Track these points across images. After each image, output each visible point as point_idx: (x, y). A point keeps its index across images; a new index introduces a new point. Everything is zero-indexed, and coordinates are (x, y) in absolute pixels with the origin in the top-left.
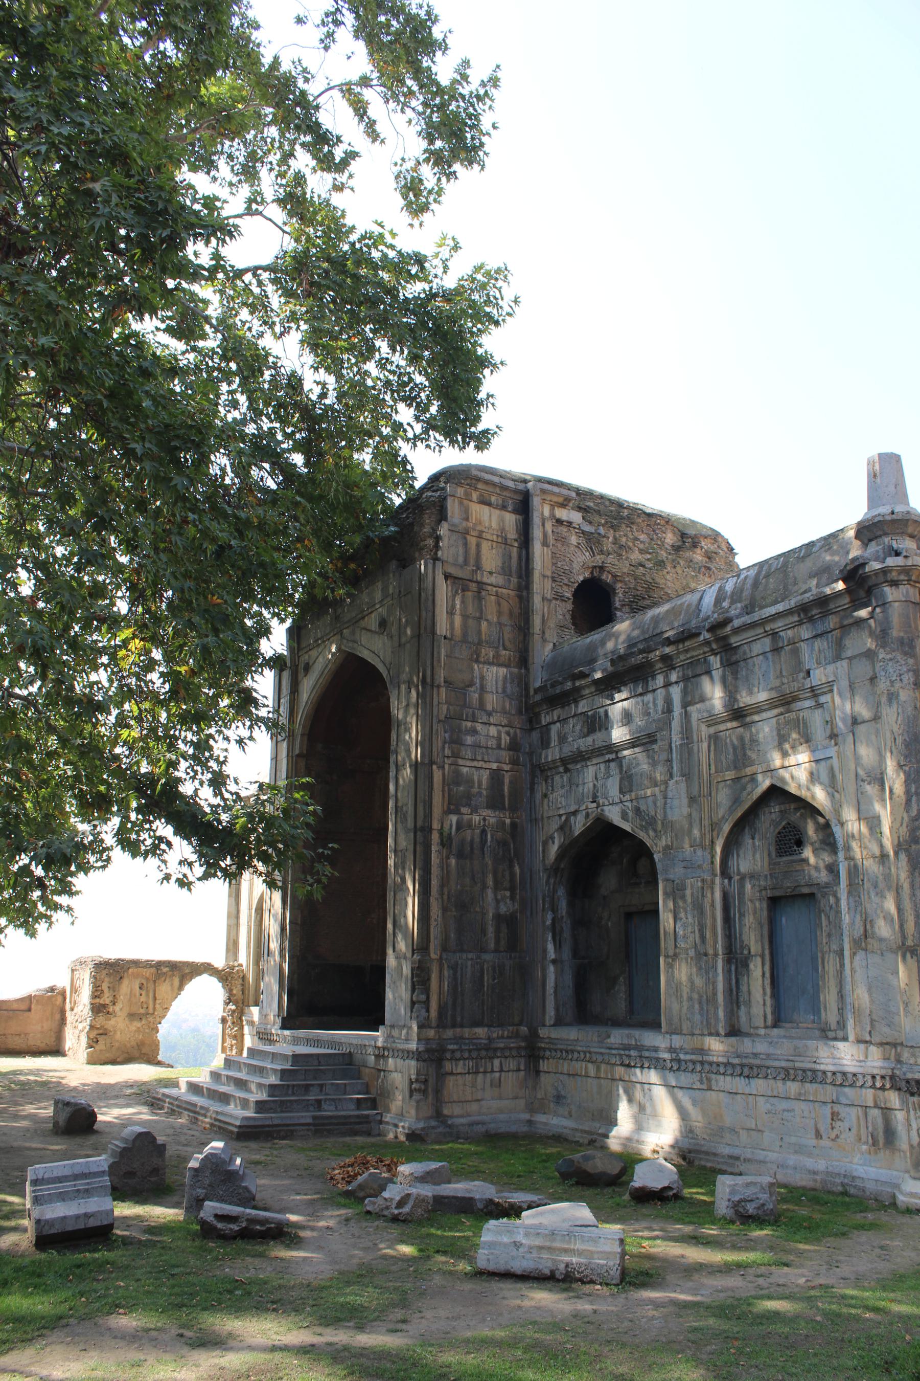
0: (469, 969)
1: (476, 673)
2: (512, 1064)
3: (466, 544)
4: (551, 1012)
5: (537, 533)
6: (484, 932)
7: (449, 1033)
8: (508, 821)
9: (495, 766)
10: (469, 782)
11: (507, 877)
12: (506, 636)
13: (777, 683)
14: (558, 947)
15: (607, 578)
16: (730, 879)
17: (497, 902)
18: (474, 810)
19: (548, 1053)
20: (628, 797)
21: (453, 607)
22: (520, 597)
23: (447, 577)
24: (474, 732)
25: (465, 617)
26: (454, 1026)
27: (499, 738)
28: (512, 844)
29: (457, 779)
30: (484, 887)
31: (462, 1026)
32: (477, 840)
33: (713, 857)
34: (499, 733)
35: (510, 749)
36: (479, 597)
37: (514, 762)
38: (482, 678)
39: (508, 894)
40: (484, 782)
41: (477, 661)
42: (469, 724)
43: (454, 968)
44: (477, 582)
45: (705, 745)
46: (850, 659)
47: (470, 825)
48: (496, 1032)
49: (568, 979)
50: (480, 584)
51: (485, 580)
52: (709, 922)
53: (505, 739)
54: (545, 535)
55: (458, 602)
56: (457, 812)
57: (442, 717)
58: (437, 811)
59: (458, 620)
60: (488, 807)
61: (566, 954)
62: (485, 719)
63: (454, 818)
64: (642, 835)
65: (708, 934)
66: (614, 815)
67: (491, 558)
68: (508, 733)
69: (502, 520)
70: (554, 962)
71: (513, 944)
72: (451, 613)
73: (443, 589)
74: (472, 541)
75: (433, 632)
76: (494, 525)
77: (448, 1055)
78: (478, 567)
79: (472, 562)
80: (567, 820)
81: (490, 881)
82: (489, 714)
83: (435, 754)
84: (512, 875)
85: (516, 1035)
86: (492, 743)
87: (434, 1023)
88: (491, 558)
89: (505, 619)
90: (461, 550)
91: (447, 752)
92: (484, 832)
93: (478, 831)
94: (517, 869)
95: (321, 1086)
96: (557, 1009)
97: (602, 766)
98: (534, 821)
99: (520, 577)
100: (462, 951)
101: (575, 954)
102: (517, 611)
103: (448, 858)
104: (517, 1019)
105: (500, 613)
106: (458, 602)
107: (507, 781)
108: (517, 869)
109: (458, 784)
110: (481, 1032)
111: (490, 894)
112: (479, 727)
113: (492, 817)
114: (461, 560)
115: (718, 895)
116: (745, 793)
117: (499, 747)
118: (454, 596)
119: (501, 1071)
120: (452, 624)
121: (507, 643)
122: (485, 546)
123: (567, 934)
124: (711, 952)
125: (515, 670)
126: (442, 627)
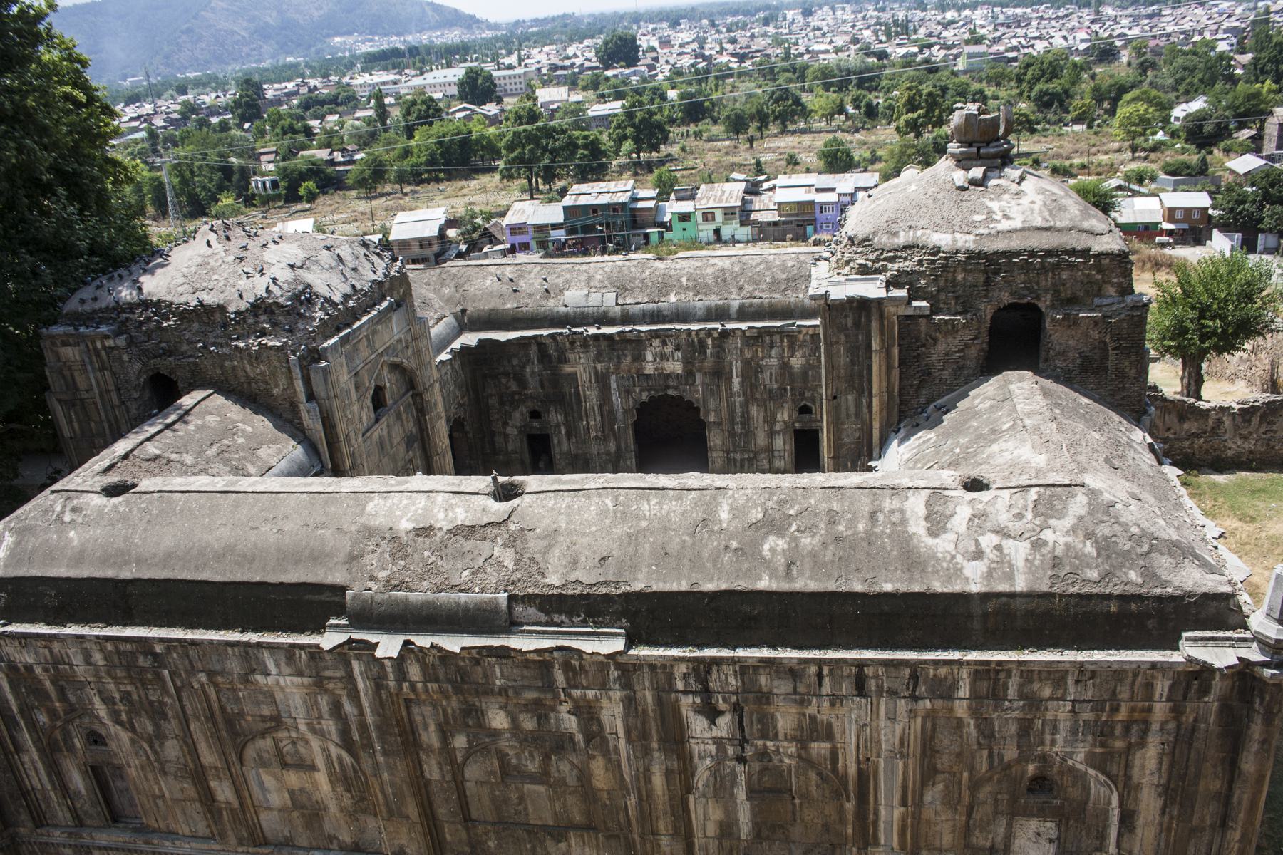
3: (64, 377)
23: (59, 401)
25: (80, 422)
50: (82, 400)
54: (102, 361)
59: (76, 425)
72: (70, 422)
74: (67, 373)
78: (77, 389)
126: (67, 432)
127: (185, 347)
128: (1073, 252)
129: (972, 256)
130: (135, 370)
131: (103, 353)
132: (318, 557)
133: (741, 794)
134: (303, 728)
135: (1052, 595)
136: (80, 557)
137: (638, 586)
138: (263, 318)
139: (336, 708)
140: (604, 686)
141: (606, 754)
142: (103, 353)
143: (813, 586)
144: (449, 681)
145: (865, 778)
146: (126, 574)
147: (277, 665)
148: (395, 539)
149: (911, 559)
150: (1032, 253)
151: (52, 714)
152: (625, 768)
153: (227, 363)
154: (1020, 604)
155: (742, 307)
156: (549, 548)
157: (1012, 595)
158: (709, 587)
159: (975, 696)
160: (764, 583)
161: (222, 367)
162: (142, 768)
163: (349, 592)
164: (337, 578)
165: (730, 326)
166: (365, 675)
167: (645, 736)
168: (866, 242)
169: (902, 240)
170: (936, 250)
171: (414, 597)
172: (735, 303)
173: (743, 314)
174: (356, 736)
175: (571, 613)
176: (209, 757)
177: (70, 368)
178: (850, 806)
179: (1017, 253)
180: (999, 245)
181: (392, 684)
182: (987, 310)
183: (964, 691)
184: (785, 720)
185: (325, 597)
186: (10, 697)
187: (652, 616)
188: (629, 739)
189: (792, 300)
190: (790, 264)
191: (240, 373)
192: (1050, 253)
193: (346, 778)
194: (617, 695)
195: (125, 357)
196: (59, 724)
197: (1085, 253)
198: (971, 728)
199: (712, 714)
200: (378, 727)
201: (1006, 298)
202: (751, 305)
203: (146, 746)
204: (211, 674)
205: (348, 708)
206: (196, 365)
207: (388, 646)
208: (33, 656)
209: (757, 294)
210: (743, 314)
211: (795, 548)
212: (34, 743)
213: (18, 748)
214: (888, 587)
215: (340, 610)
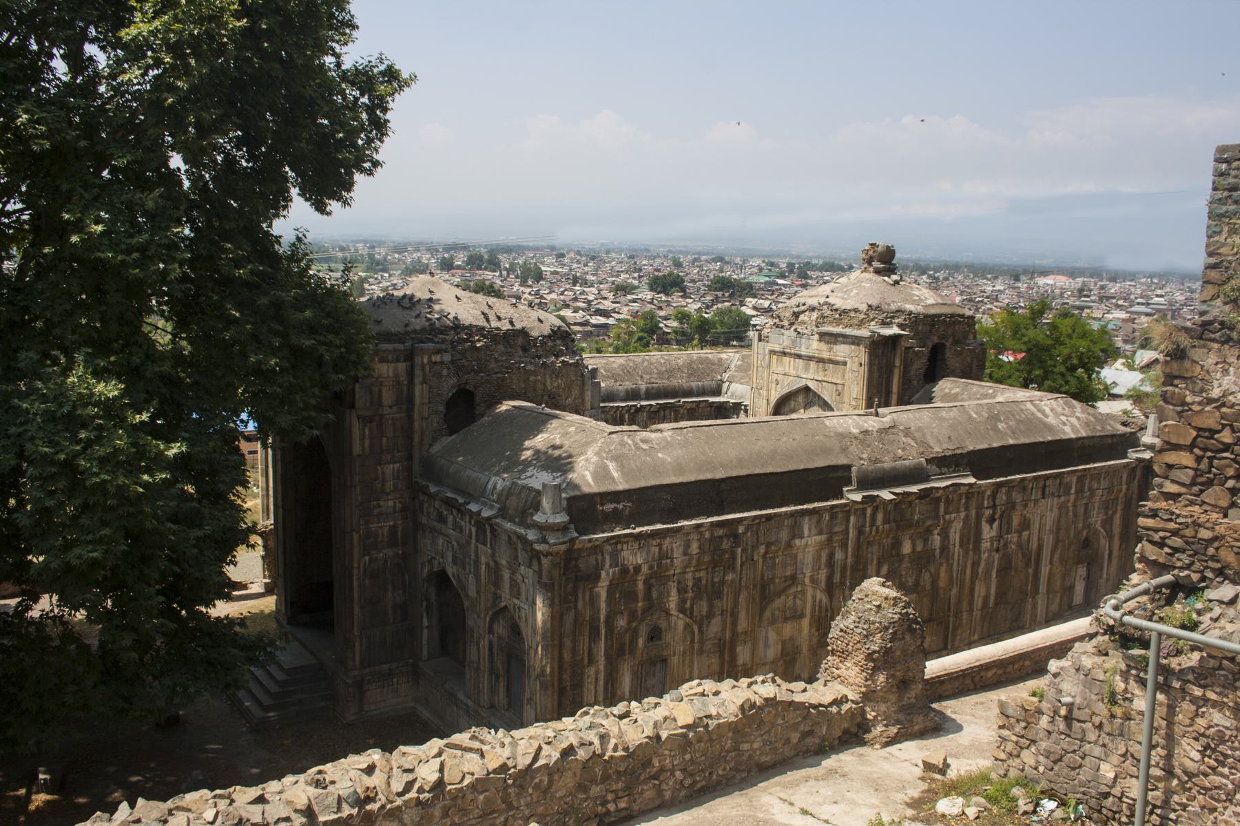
5: (418, 372)
7: (367, 671)
24: (379, 506)
38: (383, 473)
47: (377, 559)
50: (382, 416)
53: (399, 506)
54: (424, 375)
58: (356, 556)
59: (367, 442)
63: (367, 558)
67: (388, 397)
69: (396, 369)
72: (362, 439)
73: (356, 426)
74: (376, 389)
76: (391, 374)
78: (380, 404)
81: (390, 587)
82: (388, 494)
88: (388, 397)
91: (362, 522)
92: (386, 561)
110: (385, 667)
111: (390, 594)
112: (382, 503)
113: (390, 552)
115: (487, 643)
117: (395, 511)
120: (363, 446)
122: (384, 389)
126: (357, 449)
127: (493, 365)
128: (959, 315)
129: (926, 316)
130: (449, 385)
131: (427, 368)
132: (826, 451)
133: (994, 574)
134: (807, 581)
135: (1092, 437)
136: (680, 469)
137: (971, 448)
138: (559, 342)
139: (831, 556)
140: (958, 511)
141: (947, 561)
142: (427, 368)
143: (1027, 441)
144: (895, 521)
145: (1040, 547)
146: (720, 475)
147: (810, 529)
148: (856, 438)
149: (1050, 428)
150: (946, 315)
151: (632, 616)
152: (955, 568)
153: (532, 378)
154: (1087, 442)
155: (647, 389)
156: (924, 435)
157: (1083, 438)
158: (995, 445)
159: (1076, 492)
160: (1011, 442)
162: (684, 652)
163: (854, 469)
164: (843, 461)
165: (644, 403)
166: (855, 527)
167: (968, 543)
168: (878, 308)
169: (893, 307)
170: (911, 313)
171: (887, 466)
172: (643, 387)
173: (649, 395)
174: (837, 578)
175: (948, 466)
176: (743, 624)
177: (381, 384)
178: (1030, 571)
179: (940, 315)
180: (933, 311)
181: (867, 529)
182: (930, 345)
183: (1073, 491)
184: (1016, 521)
185: (839, 474)
186: (603, 605)
187: (981, 462)
188: (961, 546)
191: (540, 386)
192: (952, 316)
193: (819, 618)
194: (963, 515)
195: (445, 372)
196: (634, 624)
197: (962, 316)
198: (1071, 514)
199: (991, 521)
200: (852, 566)
201: (936, 340)
203: (696, 629)
204: (769, 545)
205: (839, 555)
206: (504, 379)
207: (886, 495)
210: (649, 395)
211: (1009, 427)
212: (606, 650)
213: (591, 661)
214: (1050, 438)
215: (849, 483)
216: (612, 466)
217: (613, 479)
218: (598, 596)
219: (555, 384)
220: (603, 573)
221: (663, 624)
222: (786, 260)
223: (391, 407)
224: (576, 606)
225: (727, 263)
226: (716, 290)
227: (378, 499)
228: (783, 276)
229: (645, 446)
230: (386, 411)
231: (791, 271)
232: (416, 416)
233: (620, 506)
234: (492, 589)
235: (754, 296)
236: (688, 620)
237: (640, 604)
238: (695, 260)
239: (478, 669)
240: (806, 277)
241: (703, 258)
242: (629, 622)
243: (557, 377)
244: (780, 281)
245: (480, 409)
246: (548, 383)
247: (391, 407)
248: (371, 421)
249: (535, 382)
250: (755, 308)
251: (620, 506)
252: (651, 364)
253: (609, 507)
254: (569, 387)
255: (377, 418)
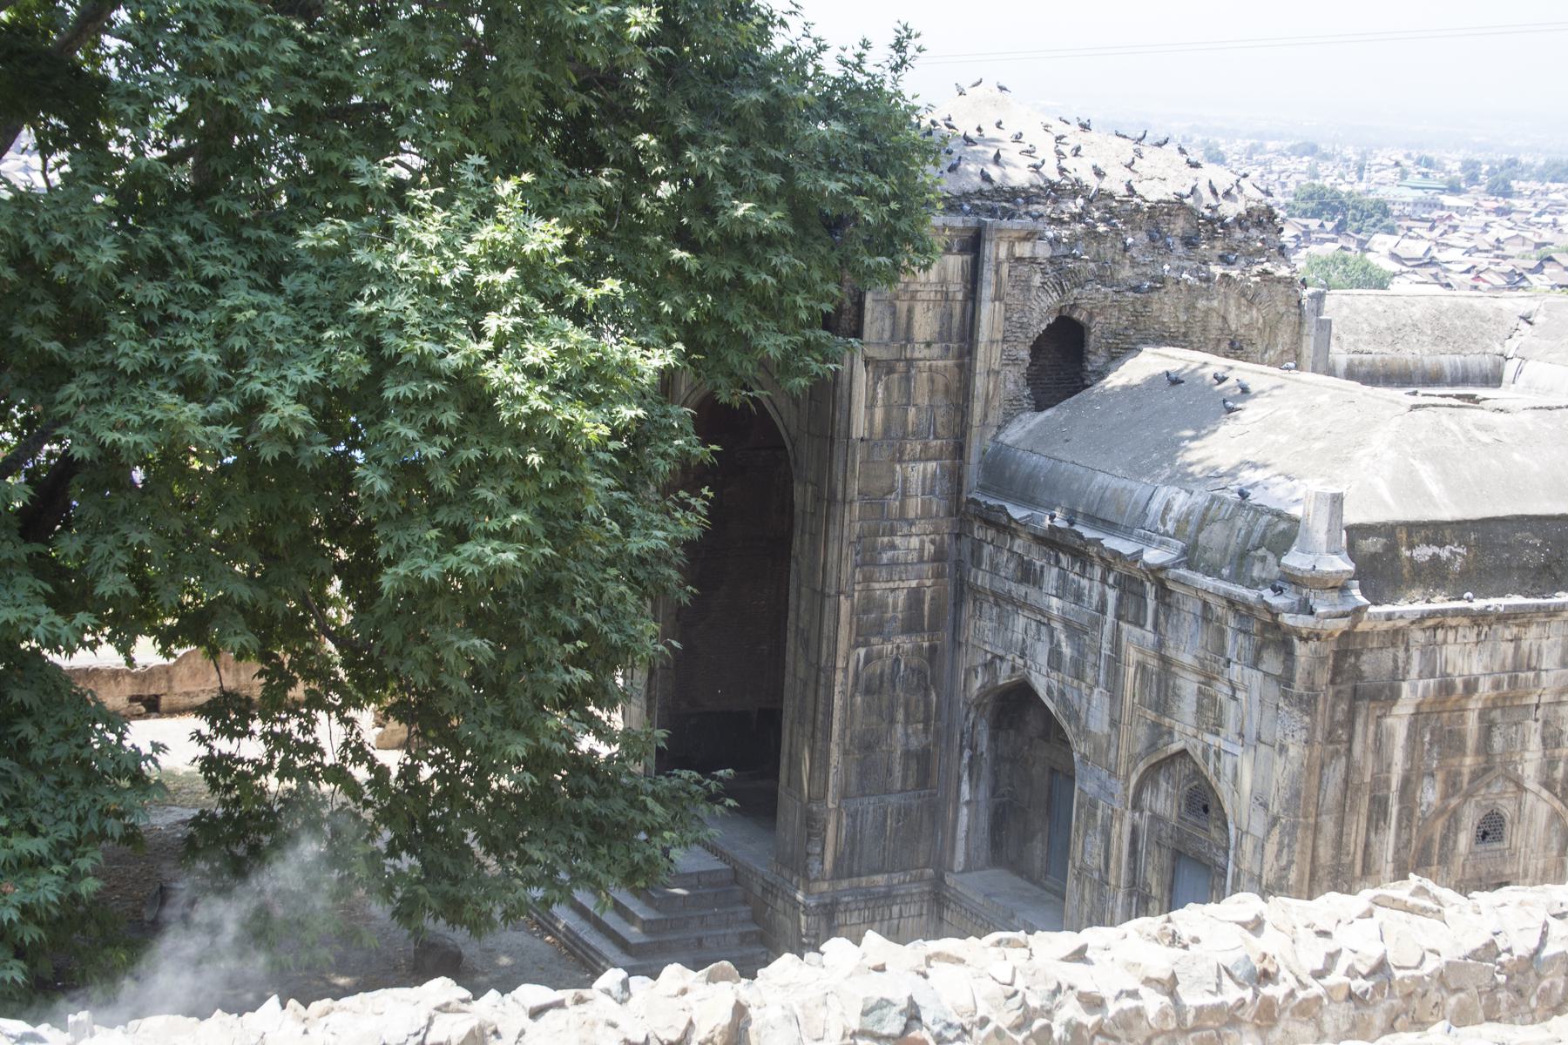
0: (870, 817)
1: (898, 477)
2: (914, 909)
3: (894, 313)
4: (960, 857)
5: (988, 275)
6: (889, 772)
7: (845, 884)
8: (926, 644)
9: (914, 584)
10: (883, 606)
11: (922, 708)
12: (939, 420)
13: (1201, 654)
14: (974, 787)
15: (1080, 316)
16: (1142, 812)
17: (907, 735)
18: (887, 639)
19: (952, 906)
20: (1054, 674)
21: (874, 398)
22: (960, 367)
24: (893, 547)
25: (888, 407)
26: (850, 875)
27: (922, 549)
28: (932, 671)
29: (869, 604)
30: (892, 721)
31: (859, 875)
32: (887, 671)
33: (1126, 789)
34: (922, 543)
35: (933, 561)
36: (907, 378)
37: (938, 575)
38: (905, 480)
39: (920, 726)
40: (900, 604)
41: (900, 461)
42: (886, 539)
43: (853, 816)
44: (906, 360)
45: (1132, 670)
46: (1266, 674)
47: (880, 657)
48: (897, 878)
49: (984, 821)
50: (910, 362)
51: (917, 355)
52: (1114, 852)
53: (929, 548)
55: (880, 390)
56: (867, 644)
57: (854, 538)
58: (842, 646)
59: (879, 414)
60: (903, 633)
61: (984, 792)
62: (905, 530)
63: (862, 651)
64: (1064, 723)
65: (1112, 865)
66: (1040, 684)
68: (933, 542)
70: (968, 803)
71: (924, 780)
72: (871, 406)
73: (862, 377)
74: (902, 306)
75: (848, 437)
77: (842, 908)
78: (909, 339)
79: (902, 335)
80: (992, 662)
81: (900, 716)
82: (911, 523)
83: (843, 583)
84: (927, 705)
85: (920, 879)
86: (913, 557)
87: (828, 876)
88: (925, 324)
89: (939, 399)
90: (888, 322)
91: (858, 577)
92: (897, 661)
93: (888, 662)
94: (934, 696)
95: (702, 918)
96: (967, 854)
97: (1034, 624)
98: (957, 644)
99: (962, 340)
100: (864, 795)
101: (994, 791)
102: (955, 385)
103: (853, 696)
104: (921, 862)
105: (932, 392)
106: (880, 390)
107: (928, 598)
108: (934, 696)
109: (866, 611)
110: (880, 879)
111: (899, 728)
112: (898, 540)
113: (906, 643)
114: (887, 335)
115: (1127, 829)
116: (1161, 742)
117: (921, 560)
118: (876, 384)
119: (901, 916)
121: (940, 429)
122: (919, 309)
123: (986, 772)
124: (1113, 882)
125: (948, 462)
126: (859, 428)
130: (1041, 311)
131: (1005, 269)
142: (1005, 269)
151: (1451, 784)
161: (1190, 308)
177: (913, 298)
189: (1409, 357)
190: (1380, 309)
191: (1215, 322)
195: (1037, 280)
202: (1361, 364)
208: (1486, 658)
209: (1361, 347)
212: (1397, 851)
216: (1426, 472)
217: (1430, 497)
218: (1391, 735)
219: (1246, 319)
220: (1405, 686)
221: (1507, 808)
222: (1461, 155)
223: (928, 345)
224: (1350, 750)
225: (1326, 157)
226: (1304, 214)
227: (892, 533)
228: (1454, 189)
229: (1485, 438)
230: (920, 352)
231: (1473, 179)
232: (980, 366)
233: (1444, 553)
234: (1151, 715)
235: (1391, 231)
236: (1558, 804)
237: (1468, 761)
238: (1253, 150)
239: (1104, 882)
240: (1507, 193)
241: (1271, 145)
242: (1445, 796)
243: (1251, 303)
244: (1448, 200)
245: (1096, 361)
246: (1232, 317)
247: (928, 345)
248: (890, 371)
249: (1207, 312)
250: (1394, 256)
251: (1444, 553)
252: (1356, 312)
253: (1423, 553)
254: (1272, 327)
255: (901, 366)
